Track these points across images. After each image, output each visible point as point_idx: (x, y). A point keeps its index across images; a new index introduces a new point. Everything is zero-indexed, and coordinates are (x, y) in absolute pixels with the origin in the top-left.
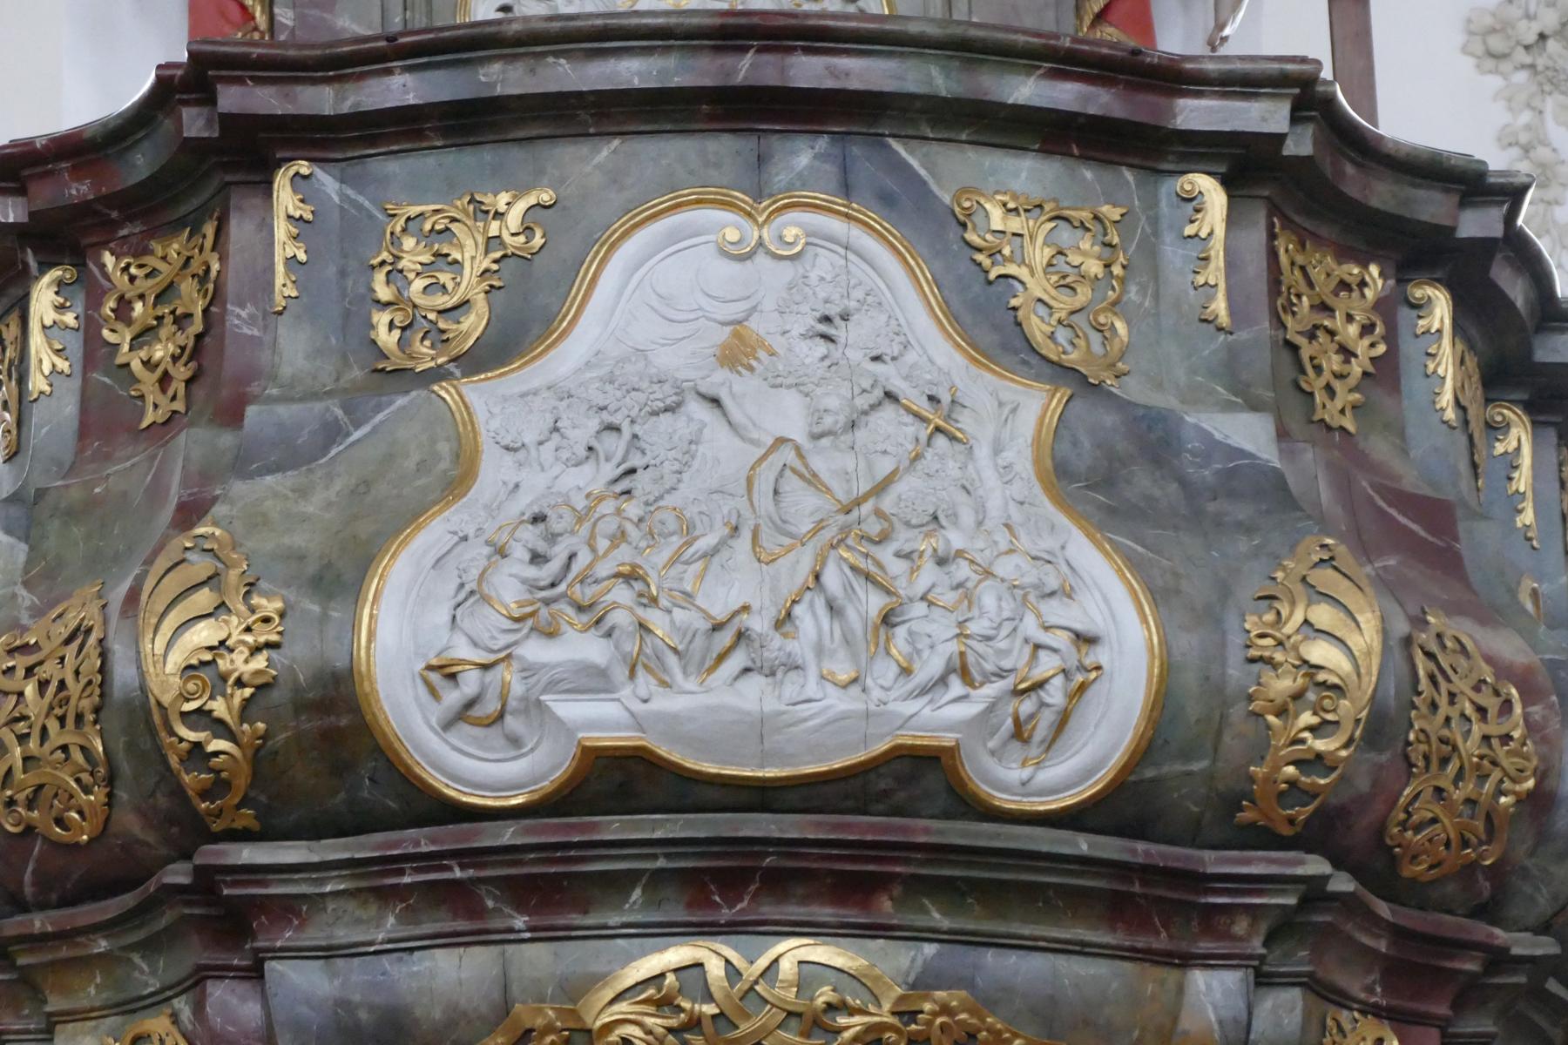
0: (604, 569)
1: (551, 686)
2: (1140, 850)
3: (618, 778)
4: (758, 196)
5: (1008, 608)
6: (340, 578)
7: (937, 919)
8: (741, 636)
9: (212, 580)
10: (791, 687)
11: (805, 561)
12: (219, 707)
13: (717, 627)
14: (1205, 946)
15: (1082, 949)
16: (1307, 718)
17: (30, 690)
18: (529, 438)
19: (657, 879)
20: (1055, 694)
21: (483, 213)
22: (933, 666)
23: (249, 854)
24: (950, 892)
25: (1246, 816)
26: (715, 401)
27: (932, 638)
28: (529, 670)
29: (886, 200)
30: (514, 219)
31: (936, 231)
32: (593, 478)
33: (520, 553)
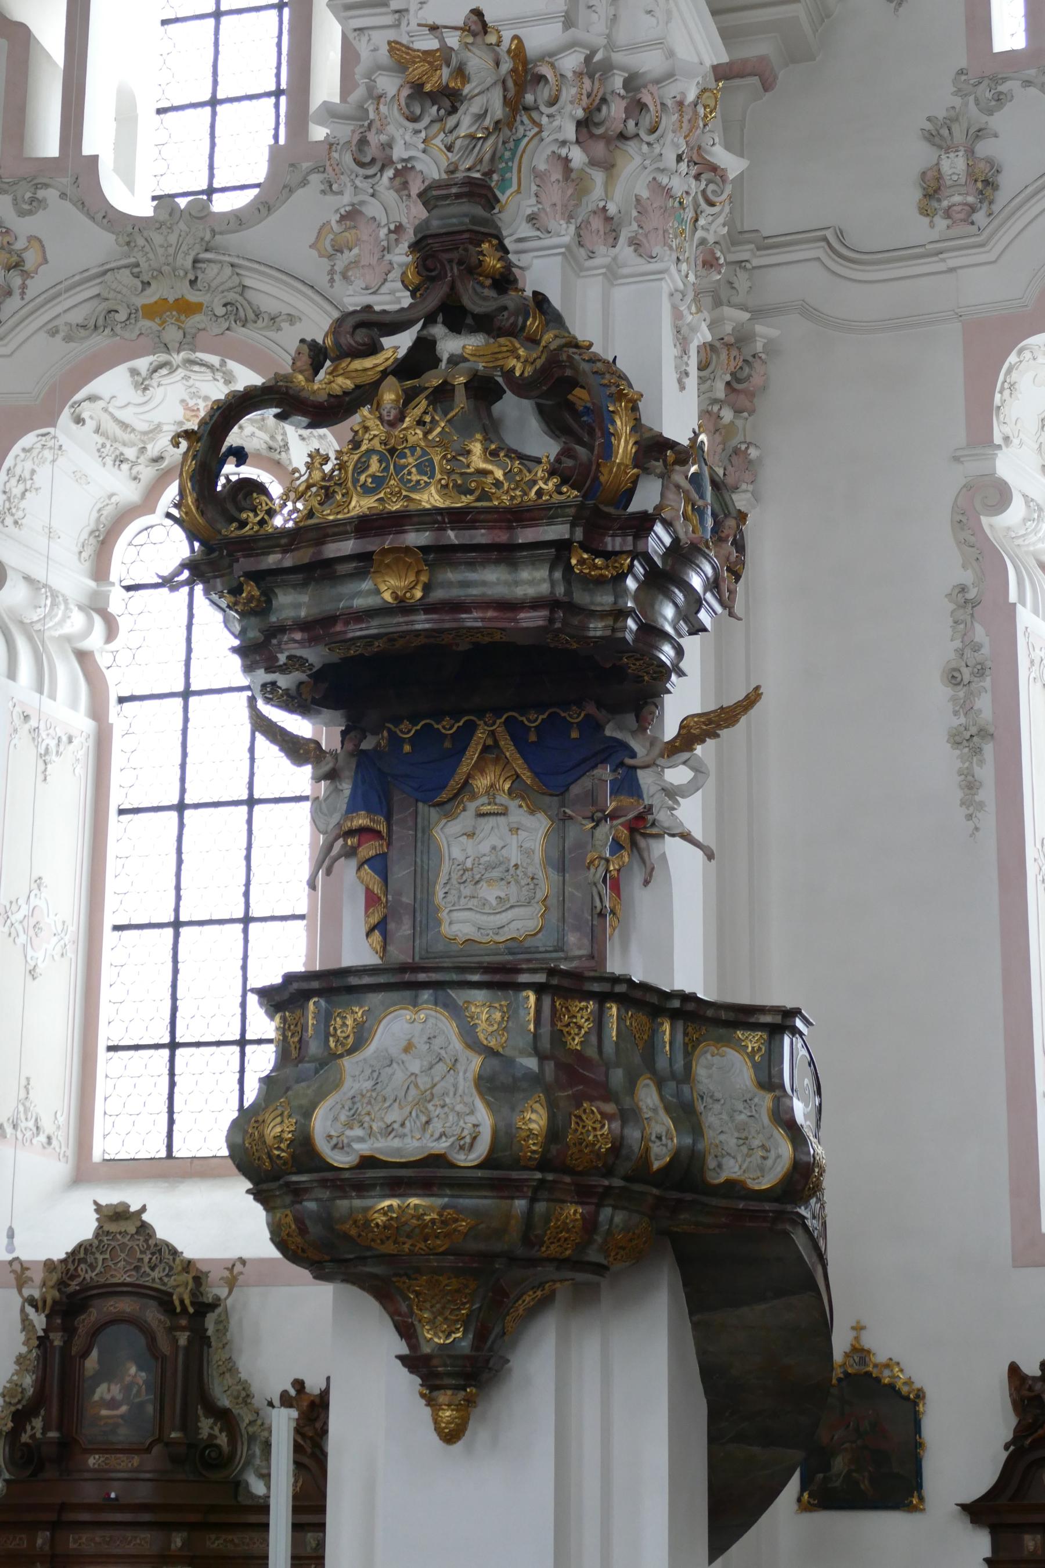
0: (363, 1113)
1: (353, 1141)
2: (496, 1174)
3: (368, 1162)
4: (414, 1006)
5: (456, 1118)
6: (308, 1114)
7: (448, 1192)
8: (393, 1129)
9: (281, 1115)
11: (408, 1109)
12: (282, 1146)
13: (388, 1126)
14: (518, 1194)
15: (485, 1197)
18: (357, 1073)
19: (382, 1185)
20: (468, 1140)
21: (353, 1012)
22: (437, 1135)
24: (451, 1186)
27: (437, 1127)
28: (348, 1137)
29: (445, 1006)
30: (360, 1014)
32: (369, 1084)
33: (347, 1108)
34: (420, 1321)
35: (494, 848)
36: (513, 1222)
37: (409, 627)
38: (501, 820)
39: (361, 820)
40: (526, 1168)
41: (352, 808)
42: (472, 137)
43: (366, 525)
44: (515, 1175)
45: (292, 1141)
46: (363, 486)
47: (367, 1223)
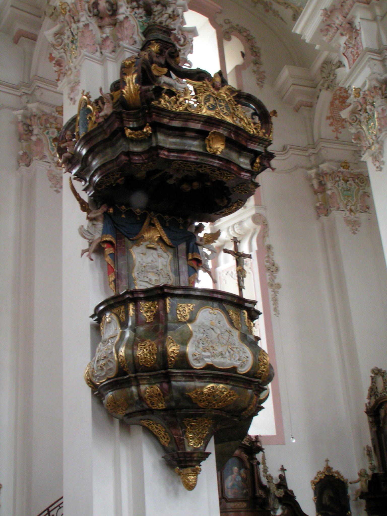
3: (209, 367)
7: (232, 383)
10: (225, 360)
16: (263, 367)
17: (145, 350)
23: (173, 371)
25: (255, 375)
26: (213, 329)
28: (203, 355)
31: (227, 313)
34: (187, 438)
35: (152, 261)
36: (247, 398)
37: (211, 164)
38: (154, 251)
39: (109, 238)
40: (256, 378)
41: (104, 232)
42: (170, 15)
43: (209, 121)
44: (253, 379)
45: (178, 354)
46: (208, 106)
47: (202, 393)
